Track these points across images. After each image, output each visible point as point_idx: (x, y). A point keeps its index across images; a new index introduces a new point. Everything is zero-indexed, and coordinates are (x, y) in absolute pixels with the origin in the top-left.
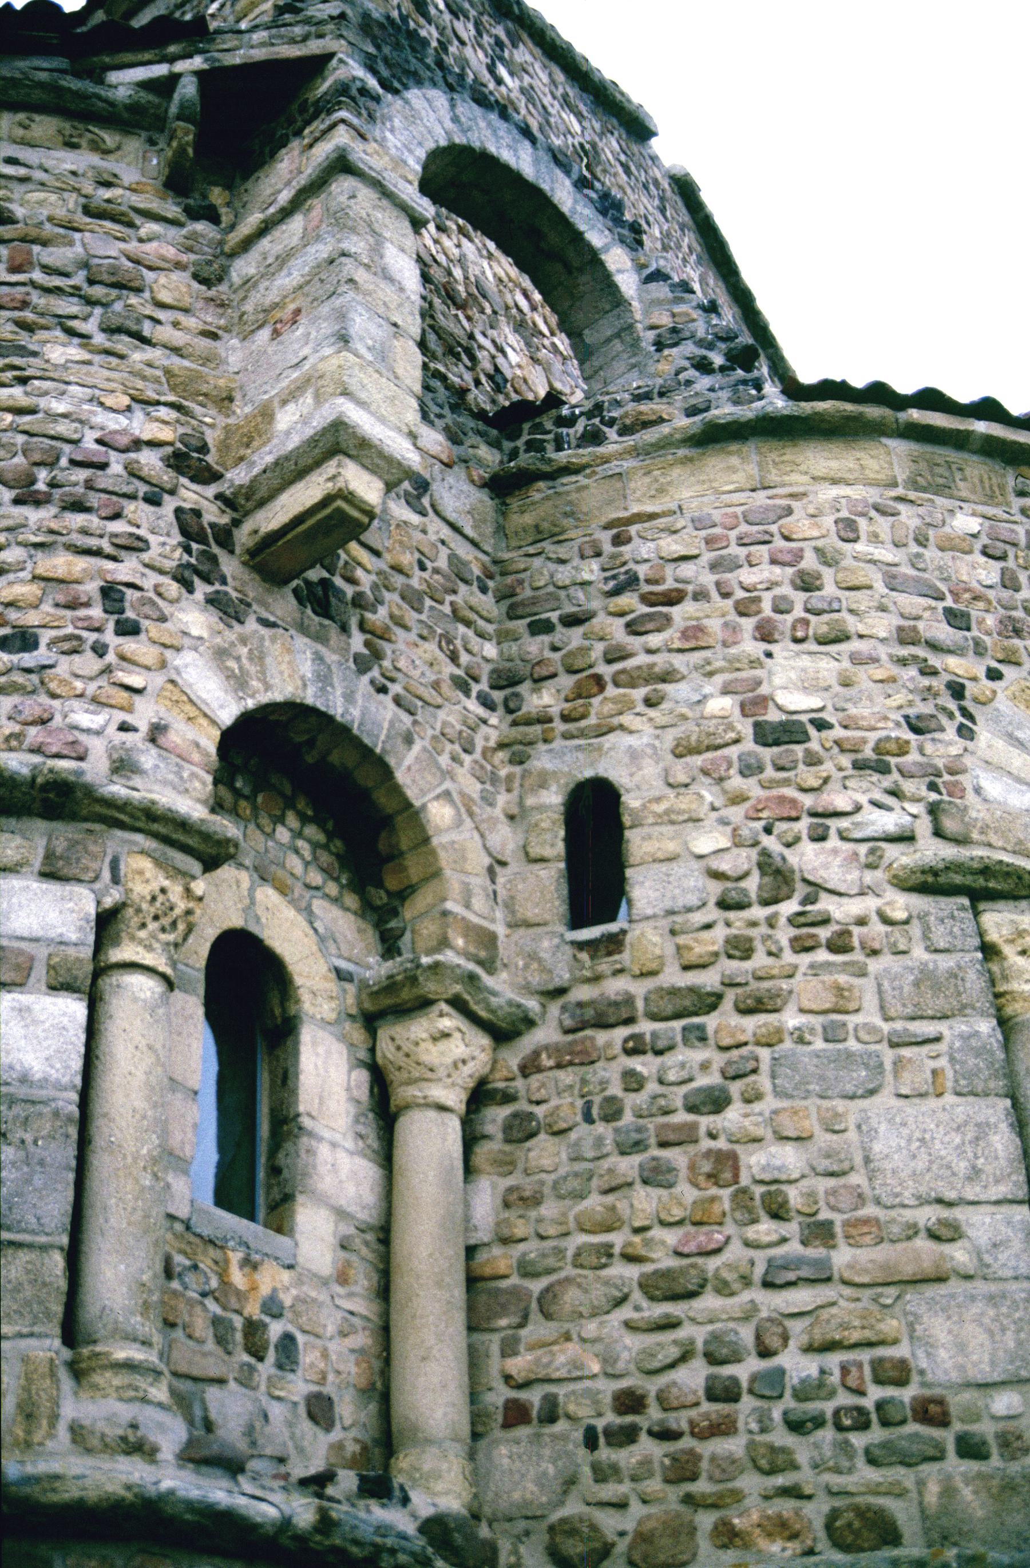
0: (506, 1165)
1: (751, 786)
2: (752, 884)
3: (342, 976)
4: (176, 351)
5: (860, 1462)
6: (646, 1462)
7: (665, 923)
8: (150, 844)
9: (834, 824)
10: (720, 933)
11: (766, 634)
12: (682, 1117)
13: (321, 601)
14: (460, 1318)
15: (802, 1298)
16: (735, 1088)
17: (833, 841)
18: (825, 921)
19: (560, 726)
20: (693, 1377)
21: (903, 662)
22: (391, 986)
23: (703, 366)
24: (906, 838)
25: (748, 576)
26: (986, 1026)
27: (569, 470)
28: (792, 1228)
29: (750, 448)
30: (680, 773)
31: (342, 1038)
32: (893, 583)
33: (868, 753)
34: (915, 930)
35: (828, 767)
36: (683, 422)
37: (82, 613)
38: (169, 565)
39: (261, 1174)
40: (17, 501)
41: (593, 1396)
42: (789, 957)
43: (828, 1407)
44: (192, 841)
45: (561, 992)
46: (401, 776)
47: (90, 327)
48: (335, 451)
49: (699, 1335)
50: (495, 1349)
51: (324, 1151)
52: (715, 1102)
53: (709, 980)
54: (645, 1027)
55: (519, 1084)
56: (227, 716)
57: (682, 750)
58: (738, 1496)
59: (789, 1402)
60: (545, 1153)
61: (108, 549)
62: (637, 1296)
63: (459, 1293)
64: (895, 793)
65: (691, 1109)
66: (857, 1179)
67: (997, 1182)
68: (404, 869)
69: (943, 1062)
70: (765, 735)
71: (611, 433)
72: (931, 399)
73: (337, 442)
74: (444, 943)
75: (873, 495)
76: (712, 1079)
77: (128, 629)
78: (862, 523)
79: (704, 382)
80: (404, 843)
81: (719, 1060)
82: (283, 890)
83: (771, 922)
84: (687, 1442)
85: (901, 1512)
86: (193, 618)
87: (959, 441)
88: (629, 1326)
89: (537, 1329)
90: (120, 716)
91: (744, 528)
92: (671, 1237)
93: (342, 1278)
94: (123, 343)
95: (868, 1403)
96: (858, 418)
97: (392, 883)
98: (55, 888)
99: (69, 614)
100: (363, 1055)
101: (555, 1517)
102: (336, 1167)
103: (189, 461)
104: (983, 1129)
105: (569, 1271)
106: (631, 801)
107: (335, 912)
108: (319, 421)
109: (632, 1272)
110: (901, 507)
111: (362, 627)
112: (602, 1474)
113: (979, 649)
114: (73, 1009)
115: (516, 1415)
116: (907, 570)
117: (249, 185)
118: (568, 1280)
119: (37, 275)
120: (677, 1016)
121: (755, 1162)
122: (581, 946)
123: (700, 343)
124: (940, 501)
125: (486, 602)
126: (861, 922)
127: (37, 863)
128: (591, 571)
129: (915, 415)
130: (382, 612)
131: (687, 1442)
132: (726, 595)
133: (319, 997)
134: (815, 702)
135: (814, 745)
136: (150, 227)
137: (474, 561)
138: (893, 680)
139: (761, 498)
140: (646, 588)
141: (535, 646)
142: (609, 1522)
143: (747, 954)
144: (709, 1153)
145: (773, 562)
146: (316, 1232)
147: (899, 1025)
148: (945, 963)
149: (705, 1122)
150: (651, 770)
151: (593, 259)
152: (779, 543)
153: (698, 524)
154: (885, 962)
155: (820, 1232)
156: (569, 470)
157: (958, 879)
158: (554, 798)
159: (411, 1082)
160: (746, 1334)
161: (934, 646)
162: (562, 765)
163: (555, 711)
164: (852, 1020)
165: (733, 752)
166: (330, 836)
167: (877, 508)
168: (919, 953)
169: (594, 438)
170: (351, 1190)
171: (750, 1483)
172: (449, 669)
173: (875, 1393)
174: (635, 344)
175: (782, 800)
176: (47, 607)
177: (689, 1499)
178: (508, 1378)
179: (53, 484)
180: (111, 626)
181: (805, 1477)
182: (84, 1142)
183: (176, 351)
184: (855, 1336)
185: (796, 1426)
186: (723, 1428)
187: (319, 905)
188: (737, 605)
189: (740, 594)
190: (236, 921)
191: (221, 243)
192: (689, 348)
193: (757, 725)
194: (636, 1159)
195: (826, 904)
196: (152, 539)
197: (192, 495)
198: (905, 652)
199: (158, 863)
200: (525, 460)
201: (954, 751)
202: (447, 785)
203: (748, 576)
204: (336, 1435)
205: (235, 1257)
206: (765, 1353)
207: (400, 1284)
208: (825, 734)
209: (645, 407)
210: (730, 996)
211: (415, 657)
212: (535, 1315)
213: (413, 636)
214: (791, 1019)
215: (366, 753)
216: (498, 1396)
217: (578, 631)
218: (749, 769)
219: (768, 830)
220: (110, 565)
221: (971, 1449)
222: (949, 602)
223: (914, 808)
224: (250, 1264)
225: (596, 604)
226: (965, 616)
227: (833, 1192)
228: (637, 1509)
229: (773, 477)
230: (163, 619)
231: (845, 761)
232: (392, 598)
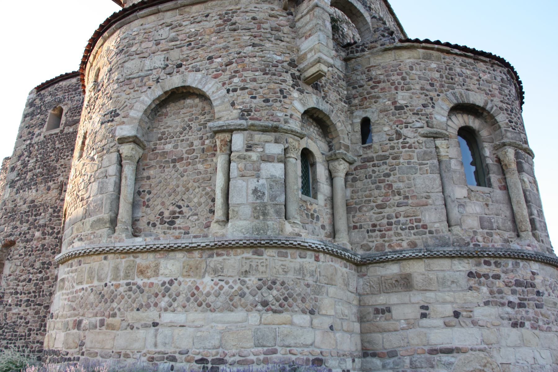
0: (352, 186)
1: (394, 118)
2: (394, 136)
3: (323, 154)
4: (288, 42)
5: (412, 235)
6: (377, 235)
7: (379, 143)
8: (293, 136)
9: (409, 125)
10: (389, 145)
11: (396, 89)
12: (383, 178)
13: (316, 87)
14: (345, 212)
15: (403, 209)
16: (392, 173)
17: (409, 128)
18: (408, 143)
19: (359, 107)
20: (385, 221)
21: (422, 94)
22: (331, 156)
23: (383, 36)
24: (422, 127)
25: (393, 78)
26: (436, 161)
27: (358, 57)
28: (402, 197)
29: (393, 51)
30: (381, 116)
31: (323, 165)
32: (420, 78)
33: (415, 112)
34: (424, 144)
35: (408, 114)
36: (379, 47)
37: (277, 95)
38: (291, 84)
39: (311, 188)
40: (264, 74)
41: (368, 225)
42: (401, 149)
43: (408, 226)
44: (298, 135)
45: (361, 156)
46: (331, 118)
47: (272, 39)
48: (319, 62)
49: (386, 214)
50: (351, 217)
51: (321, 185)
52: (388, 175)
53: (387, 153)
54: (376, 162)
55: (354, 172)
56: (302, 111)
57: (381, 111)
58: (392, 240)
59: (401, 225)
60: (359, 184)
61: (280, 82)
62: (375, 208)
63: (345, 208)
64: (420, 119)
65: (384, 176)
66: (413, 188)
67: (437, 188)
68: (332, 135)
69: (428, 168)
70: (397, 108)
71: (366, 49)
72: (427, 41)
73: (319, 61)
74: (340, 148)
75: (416, 61)
76: (388, 171)
77: (285, 97)
78: (414, 66)
79: (384, 39)
80: (332, 130)
81: (389, 168)
82: (312, 140)
83: (398, 143)
84: (384, 232)
85: (419, 242)
86: (296, 94)
87: (432, 49)
88: (374, 213)
89: (358, 214)
90: (285, 113)
91: (392, 68)
92: (381, 198)
93: (326, 206)
94: (279, 42)
95: (414, 226)
97: (330, 137)
98: (277, 145)
99: (274, 95)
100: (327, 168)
101: (362, 243)
102: (324, 188)
103: (292, 64)
104: (435, 180)
105: (364, 204)
106: (372, 120)
107: (321, 143)
108: (316, 57)
109: (374, 204)
110: (421, 63)
111: (323, 91)
112: (369, 237)
113: (436, 91)
114: (282, 165)
115: (355, 227)
116: (422, 76)
117: (298, 7)
118: (363, 206)
119: (262, 30)
120: (382, 160)
121: (395, 186)
122: (364, 147)
123: (382, 31)
124: (429, 61)
125: (344, 83)
126: (414, 143)
127: (273, 141)
128: (364, 77)
129: (424, 44)
130: (327, 88)
131: (384, 232)
132: (389, 81)
133: (319, 158)
134: (405, 102)
135: (405, 110)
136: (281, 18)
137: (342, 75)
138: (419, 97)
139: (395, 62)
140: (374, 80)
141: (354, 92)
142: (371, 244)
143: (394, 149)
144: (387, 184)
145: (398, 75)
146: (321, 198)
147: (420, 162)
148: (429, 150)
149: (387, 179)
150: (375, 114)
151: (362, 15)
152: (399, 71)
153: (383, 67)
154: (418, 150)
155: (406, 197)
156: (358, 57)
157: (431, 135)
158: (358, 120)
159: (335, 172)
160: (394, 215)
161: (427, 90)
162: (360, 114)
163: (358, 104)
164: (412, 161)
165: (391, 112)
166: (319, 129)
167: (417, 63)
168: (424, 149)
169: (363, 50)
170: (326, 191)
171: (394, 238)
172: (339, 97)
173: (415, 224)
174: (370, 31)
175: (400, 120)
176: (271, 94)
177: (384, 241)
178: (353, 222)
179: (269, 71)
180: (282, 97)
181: (403, 237)
182: (285, 187)
183: (288, 42)
184: (412, 215)
185: (402, 229)
186: (389, 230)
187: (318, 142)
188: (391, 83)
189: (391, 81)
190: (305, 146)
191: (294, 19)
192: (380, 32)
193: (395, 107)
194: (375, 185)
195: (408, 140)
196: (287, 80)
197: (294, 71)
198: (422, 92)
199: (294, 139)
200: (351, 55)
201: (431, 111)
202: (340, 119)
203: (393, 78)
204: (326, 231)
205: (308, 204)
206: (397, 218)
207: (335, 206)
208: (408, 108)
209: (372, 44)
210: (391, 156)
211: (333, 96)
212: (358, 211)
213: (332, 92)
214: (401, 160)
215: (326, 115)
216: (352, 224)
217: (361, 89)
218: (394, 115)
219: (397, 126)
220: (280, 85)
221: (431, 232)
222: (430, 82)
223: (424, 122)
224: (311, 204)
225: (364, 83)
226: (433, 84)
227: (409, 191)
228: (375, 243)
229: (397, 58)
230: (290, 95)
231: (411, 113)
232: (328, 84)
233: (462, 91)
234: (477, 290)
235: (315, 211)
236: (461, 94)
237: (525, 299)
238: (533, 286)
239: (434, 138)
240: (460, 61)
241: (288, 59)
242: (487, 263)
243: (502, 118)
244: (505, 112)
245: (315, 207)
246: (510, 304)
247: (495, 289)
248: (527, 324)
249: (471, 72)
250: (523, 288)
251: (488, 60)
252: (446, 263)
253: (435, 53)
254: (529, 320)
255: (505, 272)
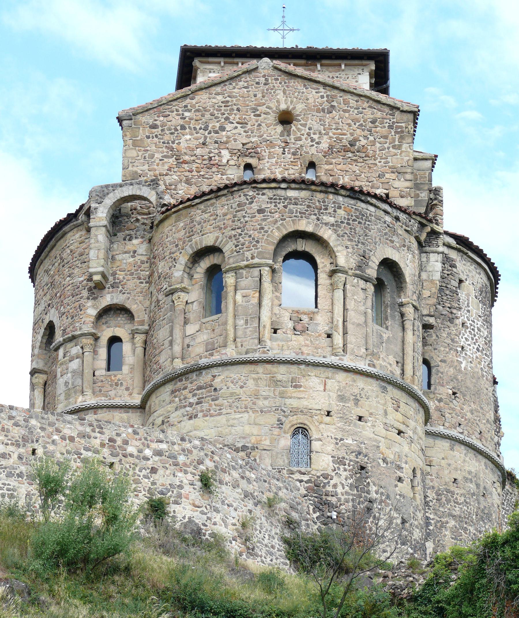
51: (127, 359)
77: (81, 310)
82: (119, 327)
86: (90, 303)
96: (167, 215)
137: (144, 258)
190: (111, 335)
211: (131, 284)
224: (115, 376)
233: (198, 238)
234: (173, 401)
235: (119, 380)
236: (196, 243)
237: (203, 398)
238: (211, 386)
239: (172, 294)
240: (203, 207)
241: (86, 277)
242: (181, 380)
243: (228, 248)
244: (233, 238)
245: (119, 377)
246: (191, 405)
247: (182, 397)
248: (200, 415)
249: (209, 214)
250: (204, 390)
251: (225, 191)
252: (162, 389)
253: (184, 212)
254: (202, 411)
255: (191, 383)
